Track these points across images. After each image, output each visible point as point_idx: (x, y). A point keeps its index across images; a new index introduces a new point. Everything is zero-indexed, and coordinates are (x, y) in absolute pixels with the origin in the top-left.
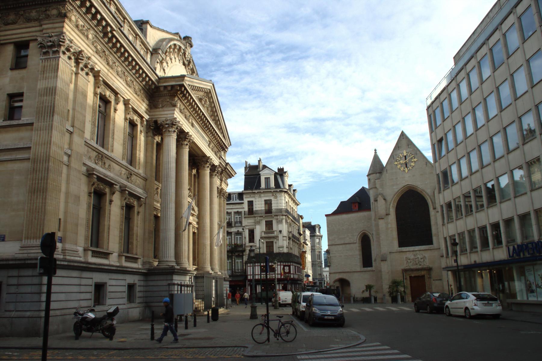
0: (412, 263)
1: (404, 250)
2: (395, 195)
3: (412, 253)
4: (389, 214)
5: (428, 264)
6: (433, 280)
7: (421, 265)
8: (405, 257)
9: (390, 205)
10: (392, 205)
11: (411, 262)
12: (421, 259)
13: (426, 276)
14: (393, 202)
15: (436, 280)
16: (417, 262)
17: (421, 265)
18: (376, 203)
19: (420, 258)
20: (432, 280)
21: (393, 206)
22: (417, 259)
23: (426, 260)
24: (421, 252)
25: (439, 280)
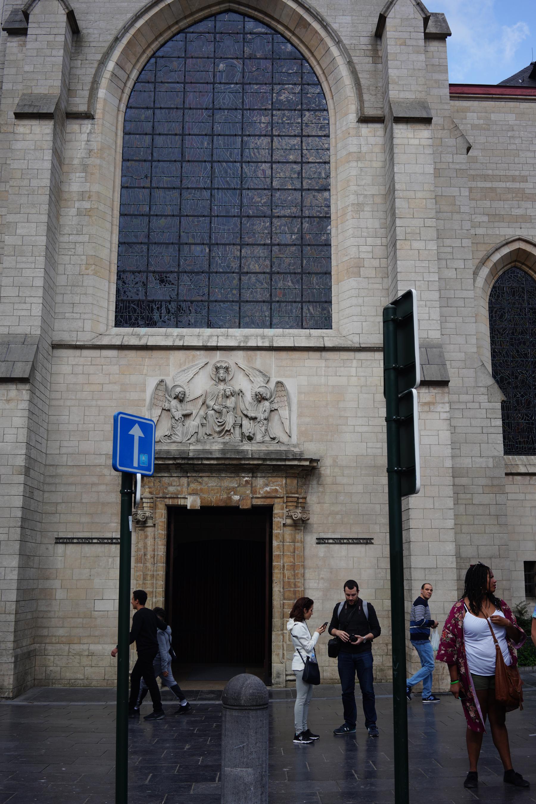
0: (193, 424)
1: (151, 342)
2: (137, 17)
3: (202, 357)
4: (88, 116)
5: (294, 440)
6: (321, 541)
7: (250, 438)
8: (152, 384)
9: (103, 63)
10: (111, 65)
11: (186, 416)
12: (260, 398)
13: (276, 511)
14: (124, 52)
15: (339, 541)
16: (230, 420)
17: (250, 438)
18: (14, 43)
19: (249, 397)
20: (311, 539)
21: (114, 74)
22: (230, 402)
23: (284, 413)
24: (260, 358)
25: (357, 541)
